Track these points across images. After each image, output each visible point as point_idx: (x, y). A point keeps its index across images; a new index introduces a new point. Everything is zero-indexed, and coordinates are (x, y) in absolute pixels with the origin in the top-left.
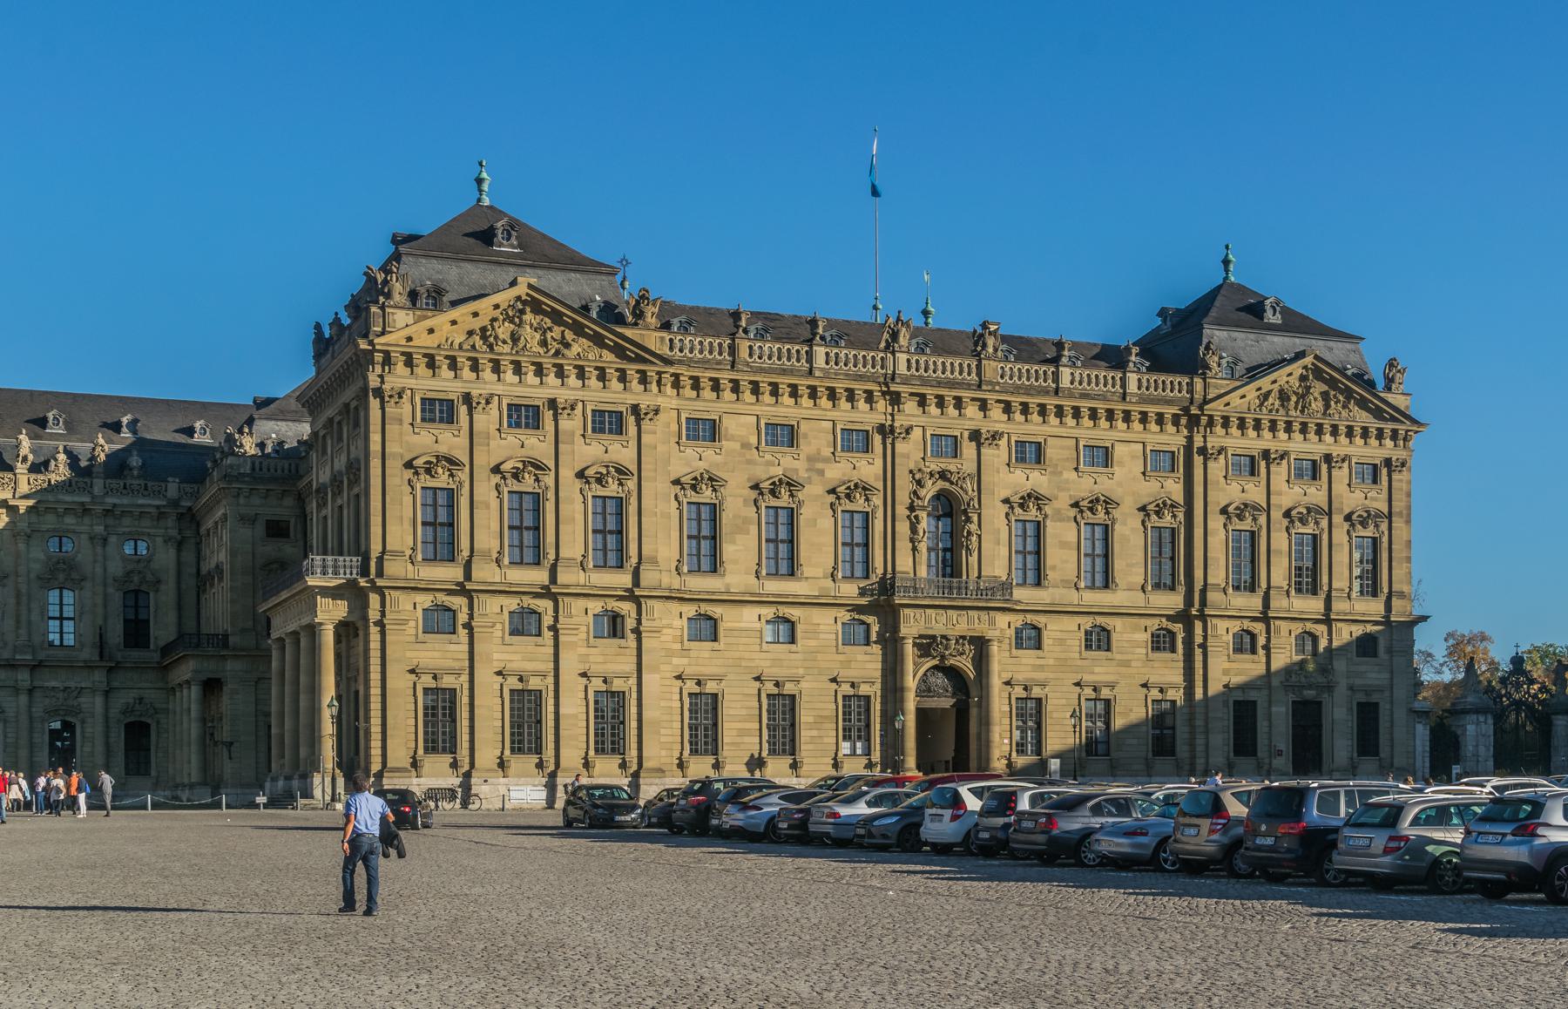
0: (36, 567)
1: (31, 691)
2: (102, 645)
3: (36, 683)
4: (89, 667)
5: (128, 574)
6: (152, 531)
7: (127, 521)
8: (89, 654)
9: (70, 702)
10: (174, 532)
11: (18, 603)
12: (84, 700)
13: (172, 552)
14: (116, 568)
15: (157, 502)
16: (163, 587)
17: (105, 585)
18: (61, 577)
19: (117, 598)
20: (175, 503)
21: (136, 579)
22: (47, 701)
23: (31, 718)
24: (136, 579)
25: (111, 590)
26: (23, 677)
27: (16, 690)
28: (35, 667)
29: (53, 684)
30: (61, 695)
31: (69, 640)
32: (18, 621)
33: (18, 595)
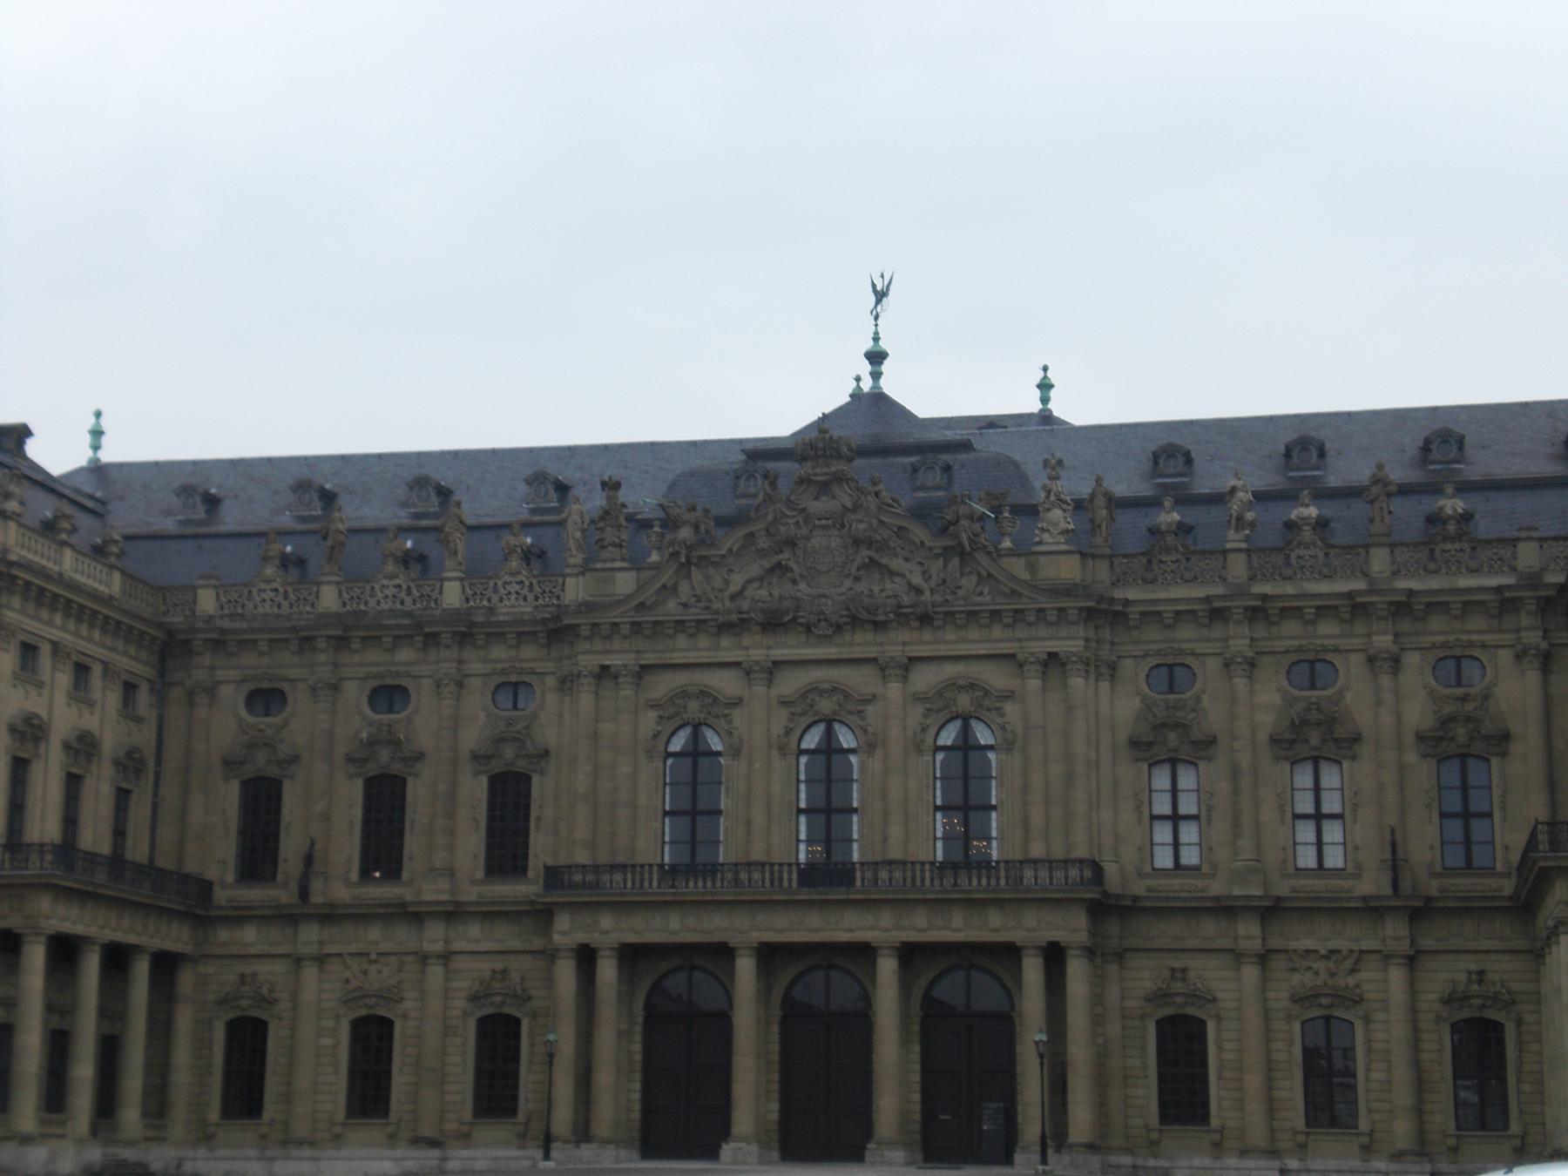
0: (1267, 721)
1: (1264, 958)
2: (1396, 865)
3: (1274, 943)
4: (1372, 910)
5: (1446, 722)
6: (1489, 638)
7: (1437, 622)
8: (1373, 883)
9: (1342, 981)
10: (1533, 638)
11: (1236, 791)
12: (1368, 976)
13: (1533, 677)
14: (1417, 714)
15: (1494, 582)
16: (1516, 748)
17: (1400, 747)
18: (1315, 738)
19: (1423, 773)
20: (1532, 581)
21: (1461, 732)
22: (1296, 979)
23: (1267, 1015)
24: (1461, 732)
25: (1411, 757)
26: (1248, 932)
27: (1237, 956)
28: (1271, 911)
29: (1307, 943)
30: (1320, 965)
31: (1334, 858)
32: (1236, 824)
33: (1235, 774)
